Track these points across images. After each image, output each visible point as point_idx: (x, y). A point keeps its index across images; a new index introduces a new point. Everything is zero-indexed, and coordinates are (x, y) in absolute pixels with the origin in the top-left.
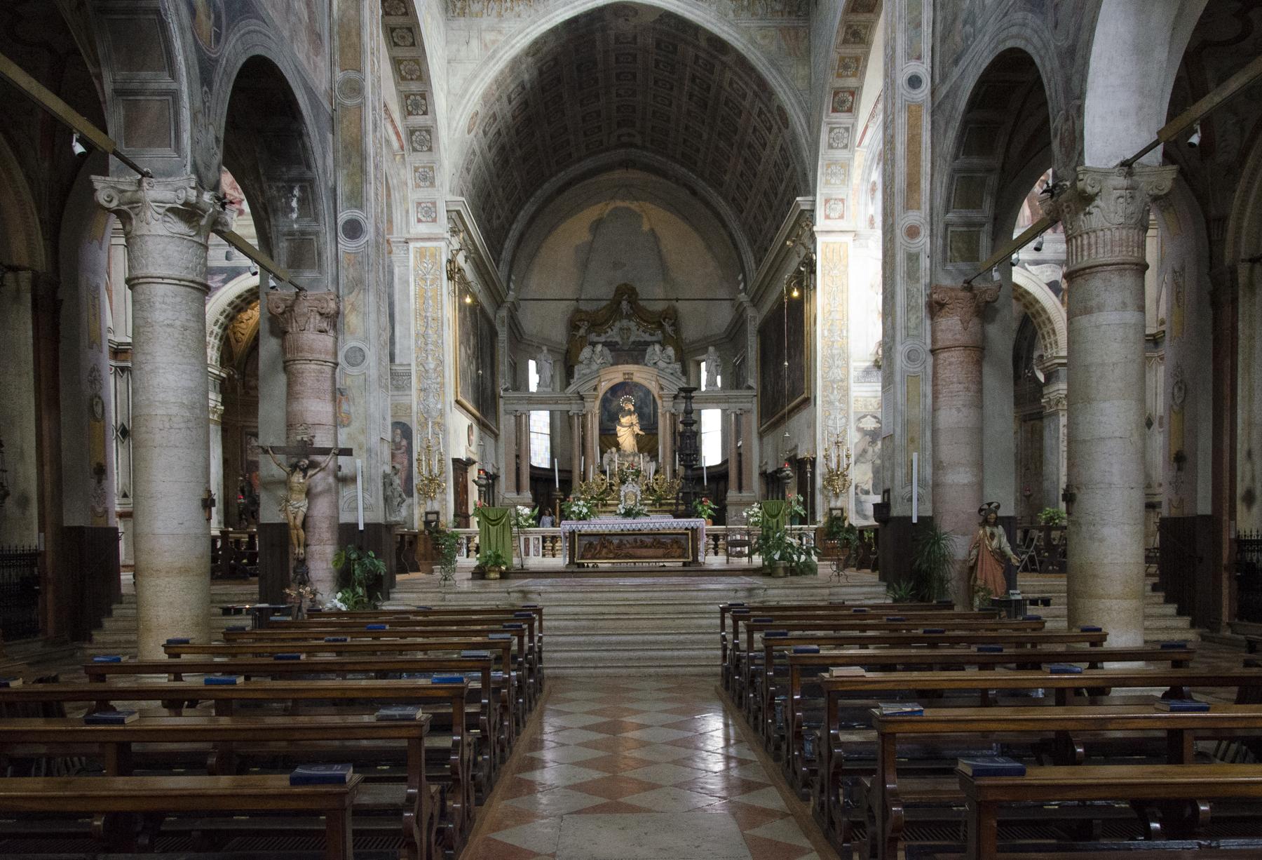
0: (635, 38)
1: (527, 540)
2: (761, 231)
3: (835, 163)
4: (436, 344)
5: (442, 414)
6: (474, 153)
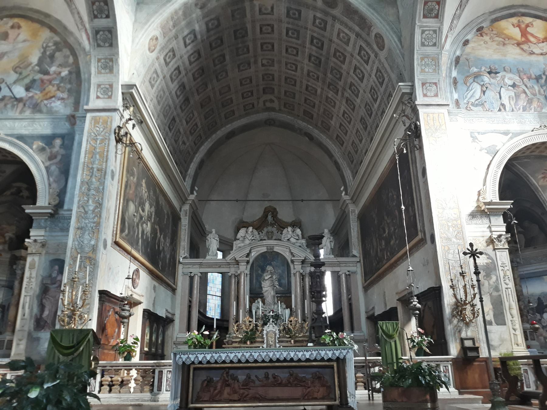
0: (272, 8)
1: (161, 373)
2: (356, 152)
3: (427, 56)
4: (97, 190)
5: (94, 249)
6: (156, 72)
